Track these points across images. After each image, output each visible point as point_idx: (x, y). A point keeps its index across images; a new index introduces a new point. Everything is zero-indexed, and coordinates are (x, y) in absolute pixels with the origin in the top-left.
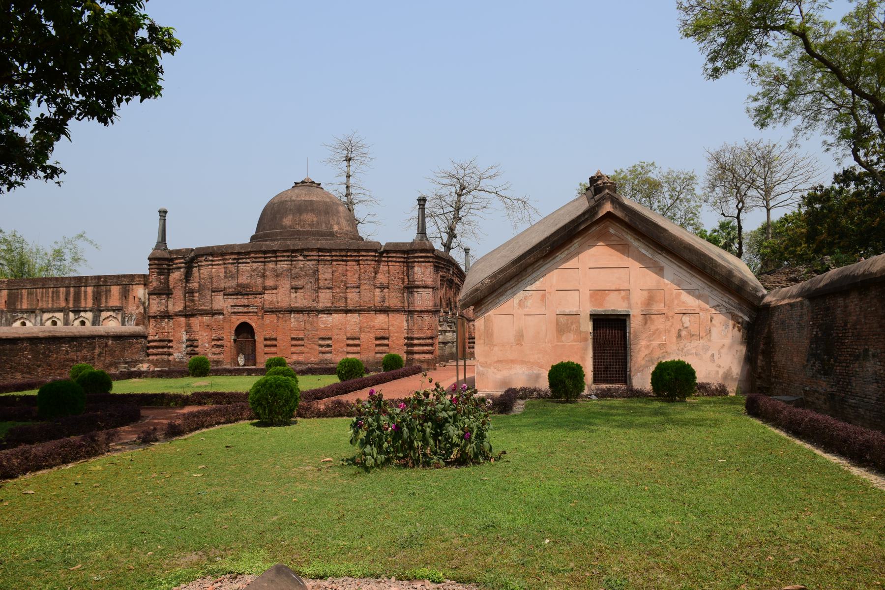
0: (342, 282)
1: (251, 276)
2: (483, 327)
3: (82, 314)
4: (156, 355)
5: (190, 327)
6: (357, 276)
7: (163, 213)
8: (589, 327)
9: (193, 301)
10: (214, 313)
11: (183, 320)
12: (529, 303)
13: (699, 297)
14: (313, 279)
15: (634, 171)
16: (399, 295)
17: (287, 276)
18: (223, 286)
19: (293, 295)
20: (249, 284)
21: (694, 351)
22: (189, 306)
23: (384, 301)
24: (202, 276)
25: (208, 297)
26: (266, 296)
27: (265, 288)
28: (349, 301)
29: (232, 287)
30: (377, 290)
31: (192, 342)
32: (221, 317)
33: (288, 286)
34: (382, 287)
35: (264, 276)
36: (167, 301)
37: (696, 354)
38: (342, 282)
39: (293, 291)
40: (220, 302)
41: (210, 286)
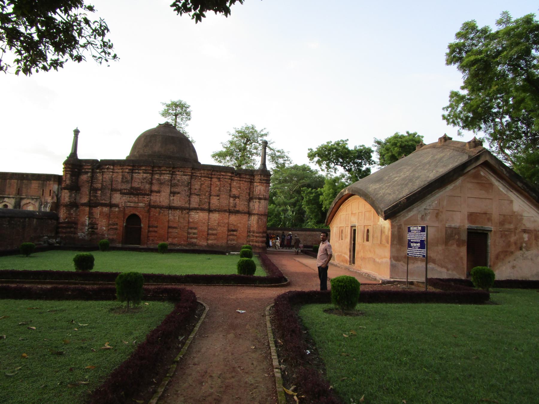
0: (207, 192)
1: (142, 182)
3: (6, 200)
4: (65, 233)
5: (93, 215)
6: (217, 189)
7: (77, 132)
8: (464, 237)
9: (96, 196)
10: (111, 206)
11: (87, 209)
12: (428, 217)
14: (186, 189)
15: (338, 144)
16: (246, 203)
17: (168, 185)
18: (119, 187)
19: (172, 198)
20: (140, 188)
21: (529, 257)
22: (92, 200)
23: (235, 207)
24: (104, 180)
25: (108, 195)
26: (152, 198)
27: (152, 191)
28: (211, 205)
29: (126, 189)
30: (231, 199)
31: (93, 226)
32: (117, 209)
33: (169, 191)
34: (235, 197)
35: (151, 183)
36: (75, 195)
37: (531, 259)
38: (207, 192)
39: (172, 195)
40: (117, 198)
41: (110, 187)
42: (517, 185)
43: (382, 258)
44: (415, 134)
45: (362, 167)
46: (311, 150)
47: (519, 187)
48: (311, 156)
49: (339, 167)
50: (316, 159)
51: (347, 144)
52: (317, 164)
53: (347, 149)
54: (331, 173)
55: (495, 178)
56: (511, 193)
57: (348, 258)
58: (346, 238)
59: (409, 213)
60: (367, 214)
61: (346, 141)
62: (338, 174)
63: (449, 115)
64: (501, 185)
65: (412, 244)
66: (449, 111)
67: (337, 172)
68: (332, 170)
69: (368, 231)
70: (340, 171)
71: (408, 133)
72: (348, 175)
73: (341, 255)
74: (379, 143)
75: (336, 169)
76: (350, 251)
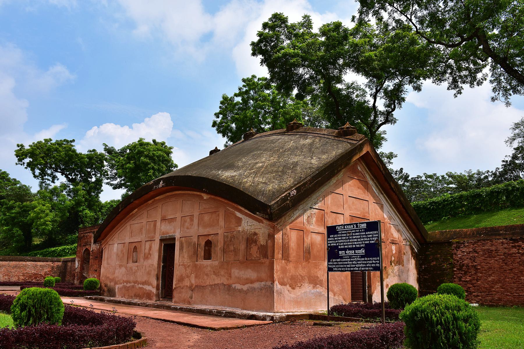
2: (281, 241)
13: (398, 231)
15: (59, 143)
42: (390, 185)
43: (252, 282)
44: (163, 144)
45: (91, 178)
46: (22, 146)
47: (391, 188)
48: (21, 154)
49: (58, 175)
50: (27, 160)
51: (72, 146)
52: (29, 169)
53: (74, 151)
54: (48, 182)
55: (369, 175)
56: (381, 195)
57: (154, 291)
58: (147, 257)
59: (295, 213)
60: (206, 218)
61: (71, 141)
62: (58, 184)
63: (221, 123)
64: (374, 185)
65: (340, 252)
66: (220, 118)
67: (56, 181)
68: (49, 178)
69: (209, 244)
70: (60, 181)
71: (154, 141)
72: (71, 187)
73: (133, 287)
74: (110, 151)
75: (54, 178)
76: (158, 279)
